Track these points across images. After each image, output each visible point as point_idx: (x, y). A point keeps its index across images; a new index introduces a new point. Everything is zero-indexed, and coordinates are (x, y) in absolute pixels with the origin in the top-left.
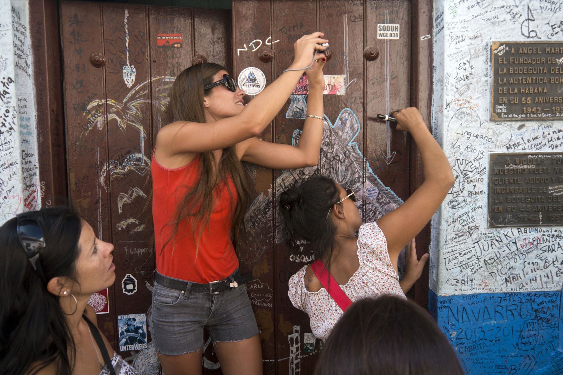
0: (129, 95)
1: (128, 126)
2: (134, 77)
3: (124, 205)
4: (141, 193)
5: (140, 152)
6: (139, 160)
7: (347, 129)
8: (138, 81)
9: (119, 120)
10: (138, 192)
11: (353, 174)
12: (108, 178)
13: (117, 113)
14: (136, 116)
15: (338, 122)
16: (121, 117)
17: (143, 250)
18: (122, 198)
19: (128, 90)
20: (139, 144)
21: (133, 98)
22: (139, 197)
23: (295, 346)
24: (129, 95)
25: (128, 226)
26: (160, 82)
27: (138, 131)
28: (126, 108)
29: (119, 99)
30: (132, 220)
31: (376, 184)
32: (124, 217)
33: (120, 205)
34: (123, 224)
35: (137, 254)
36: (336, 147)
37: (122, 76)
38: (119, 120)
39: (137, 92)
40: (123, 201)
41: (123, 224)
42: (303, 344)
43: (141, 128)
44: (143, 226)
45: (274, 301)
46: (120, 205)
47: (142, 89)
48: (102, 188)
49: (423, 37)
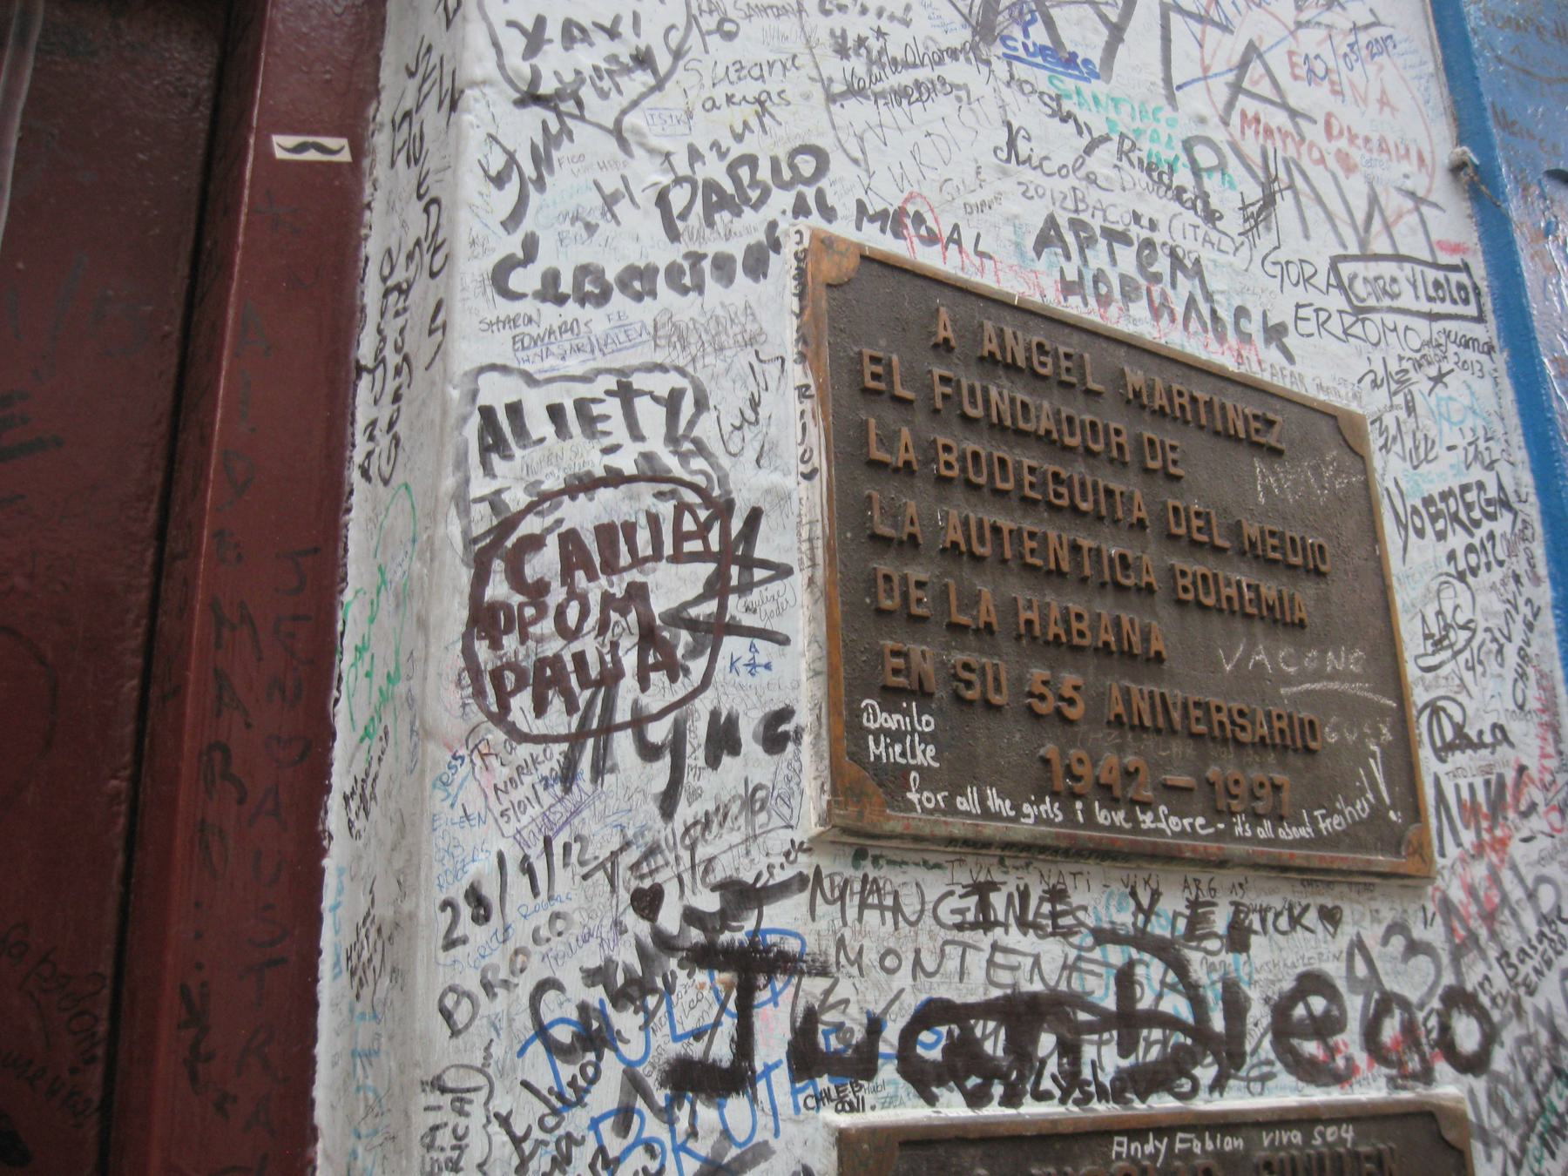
49: (292, 141)
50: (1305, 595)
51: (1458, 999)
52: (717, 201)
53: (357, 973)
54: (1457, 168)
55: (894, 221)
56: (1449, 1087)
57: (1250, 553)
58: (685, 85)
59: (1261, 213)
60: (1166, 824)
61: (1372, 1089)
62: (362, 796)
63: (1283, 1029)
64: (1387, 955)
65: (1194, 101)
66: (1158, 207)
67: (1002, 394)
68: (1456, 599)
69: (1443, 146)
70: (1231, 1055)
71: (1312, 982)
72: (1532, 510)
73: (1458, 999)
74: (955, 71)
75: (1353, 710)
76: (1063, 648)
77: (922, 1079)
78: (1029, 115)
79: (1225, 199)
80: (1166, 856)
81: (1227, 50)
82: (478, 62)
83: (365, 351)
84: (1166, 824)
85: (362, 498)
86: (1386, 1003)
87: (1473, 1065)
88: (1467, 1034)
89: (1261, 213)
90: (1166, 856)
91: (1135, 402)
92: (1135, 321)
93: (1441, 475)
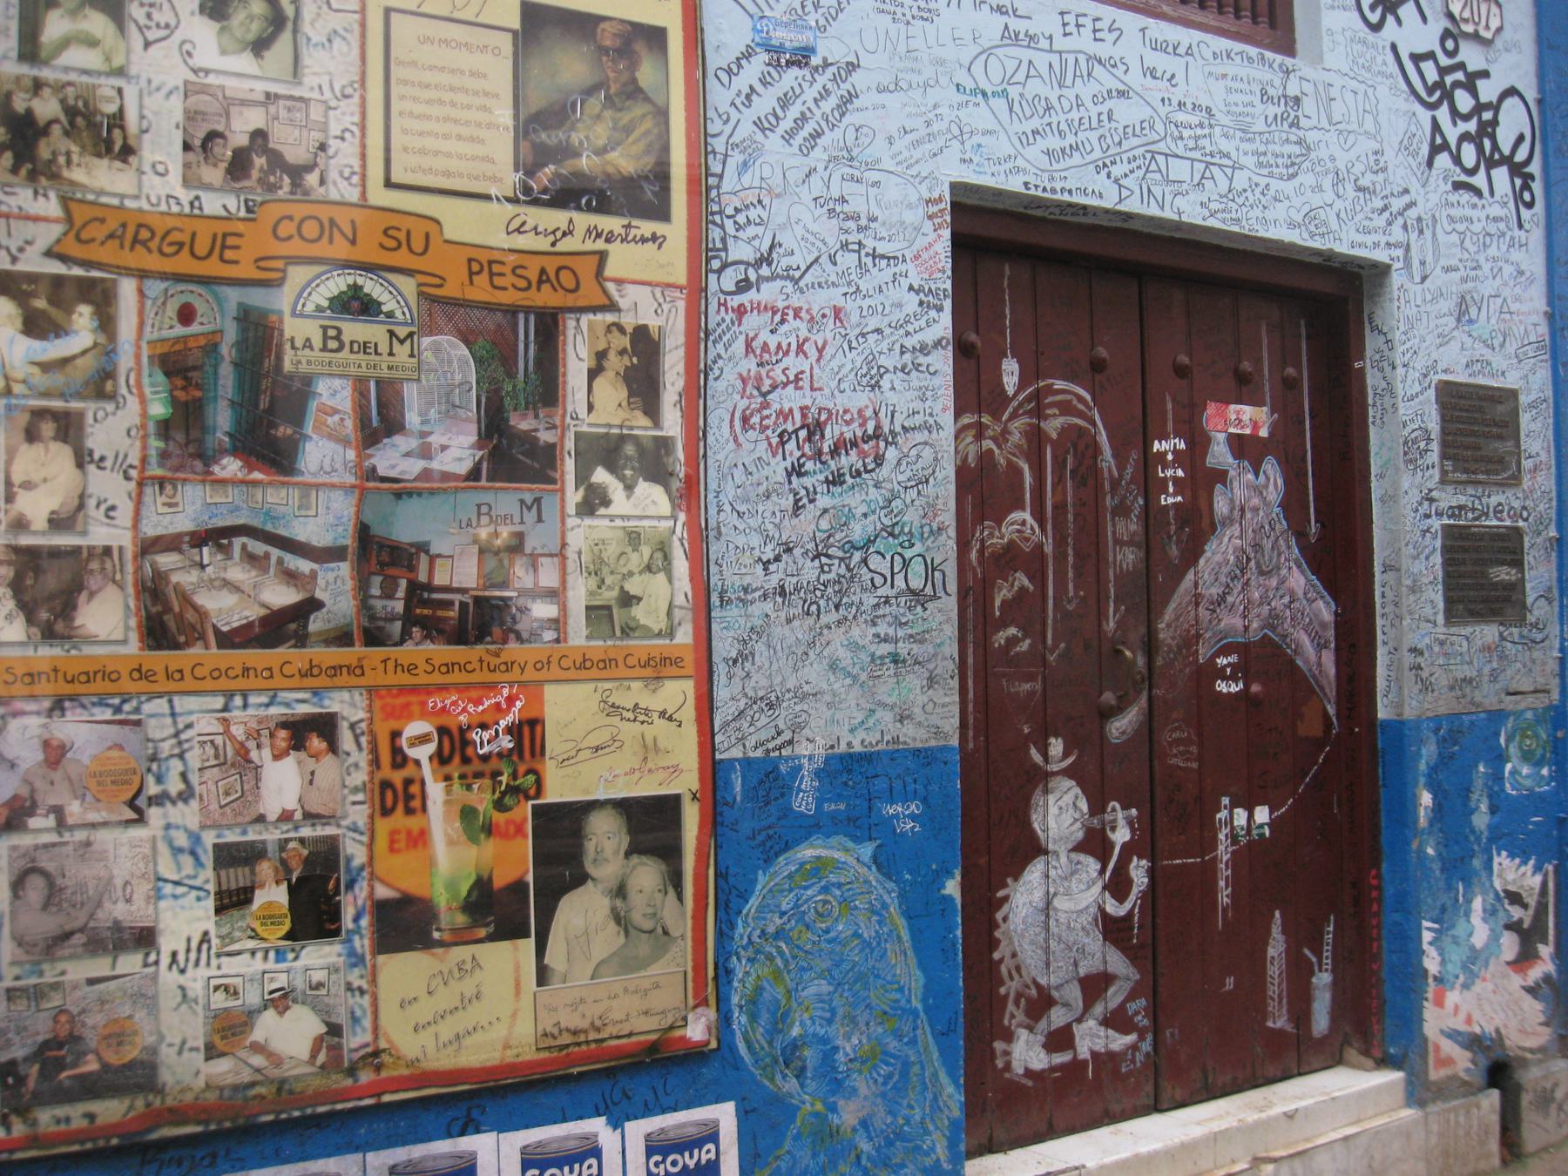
0: (1010, 409)
1: (1010, 464)
2: (1016, 379)
3: (1003, 602)
4: (1026, 582)
5: (1023, 509)
6: (1024, 523)
7: (1271, 487)
8: (1022, 386)
9: (997, 451)
10: (1022, 580)
11: (1279, 555)
12: (981, 551)
13: (994, 439)
14: (1018, 446)
15: (1262, 477)
16: (999, 447)
17: (1027, 686)
18: (1000, 589)
19: (1007, 400)
20: (1023, 495)
21: (1014, 416)
22: (1022, 589)
23: (1224, 831)
24: (1010, 409)
25: (1008, 639)
26: (1050, 390)
27: (1020, 472)
28: (1005, 432)
29: (996, 416)
30: (1012, 631)
31: (1302, 572)
32: (1003, 624)
33: (997, 603)
34: (1000, 638)
35: (1017, 693)
36: (1261, 513)
37: (1000, 376)
38: (997, 451)
39: (1021, 405)
40: (1002, 594)
41: (1000, 638)
42: (1233, 828)
43: (1026, 468)
44: (1028, 641)
45: (1200, 758)
46: (997, 603)
47: (1028, 399)
48: (974, 569)
50: (1504, 431)
51: (1524, 508)
52: (1425, 376)
53: (1382, 500)
54: (1546, 313)
55: (1445, 371)
56: (1521, 524)
57: (1496, 425)
58: (1421, 354)
59: (1502, 345)
60: (1481, 477)
61: (1508, 523)
62: (1381, 476)
63: (1495, 512)
64: (1512, 499)
65: (1493, 321)
66: (1485, 351)
67: (1463, 402)
68: (1533, 426)
69: (1545, 308)
70: (1487, 515)
71: (1500, 504)
72: (1551, 401)
73: (1524, 508)
74: (1455, 333)
75: (1510, 453)
76: (1467, 448)
77: (1449, 517)
78: (1465, 338)
79: (1496, 343)
80: (1480, 482)
81: (1499, 301)
82: (1398, 362)
83: (1370, 401)
84: (1481, 477)
85: (1372, 431)
86: (1512, 508)
87: (1526, 520)
88: (1525, 514)
89: (1502, 345)
90: (1480, 482)
91: (1480, 398)
92: (1481, 381)
93: (1532, 397)
